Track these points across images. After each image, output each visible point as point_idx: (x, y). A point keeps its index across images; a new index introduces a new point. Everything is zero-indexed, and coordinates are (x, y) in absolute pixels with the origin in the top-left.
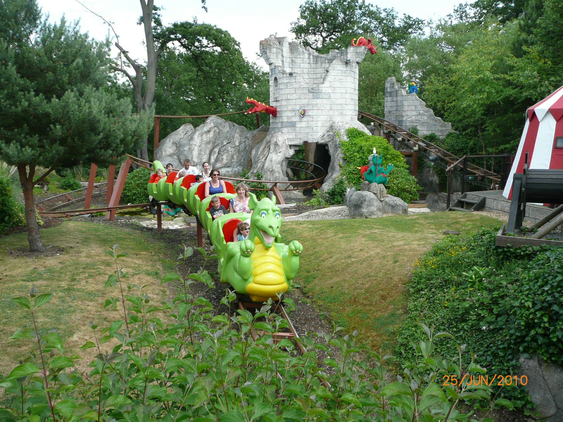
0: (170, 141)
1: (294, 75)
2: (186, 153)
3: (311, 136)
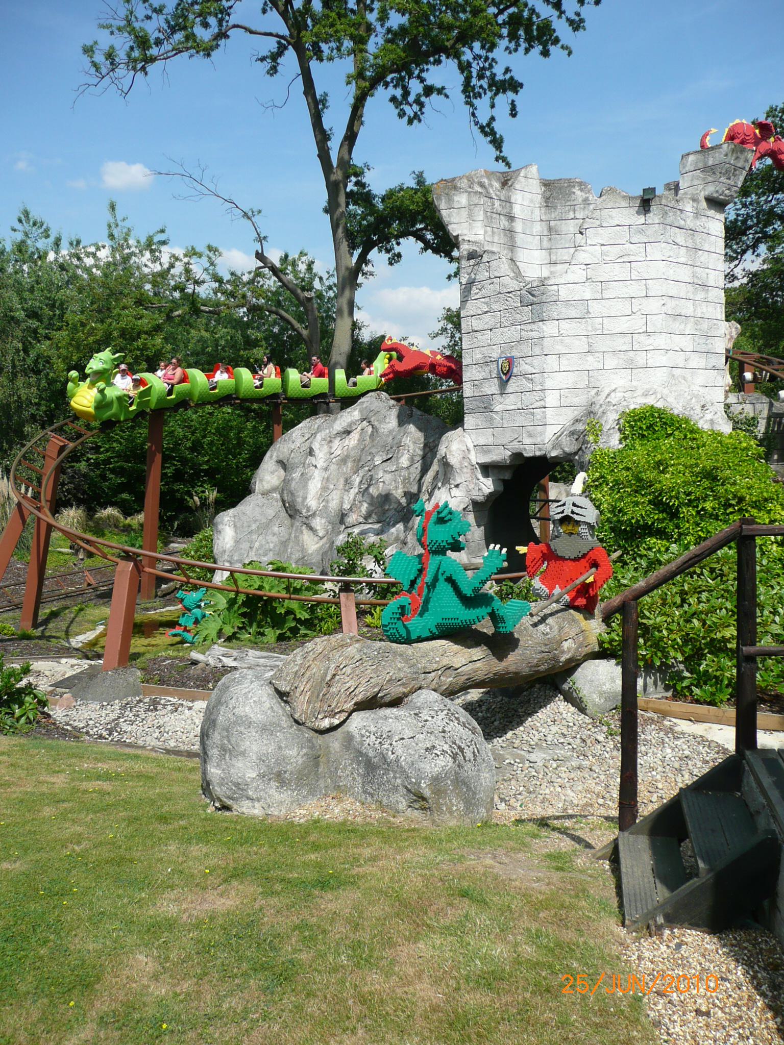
0: (271, 457)
1: (485, 258)
2: (293, 484)
3: (530, 436)
